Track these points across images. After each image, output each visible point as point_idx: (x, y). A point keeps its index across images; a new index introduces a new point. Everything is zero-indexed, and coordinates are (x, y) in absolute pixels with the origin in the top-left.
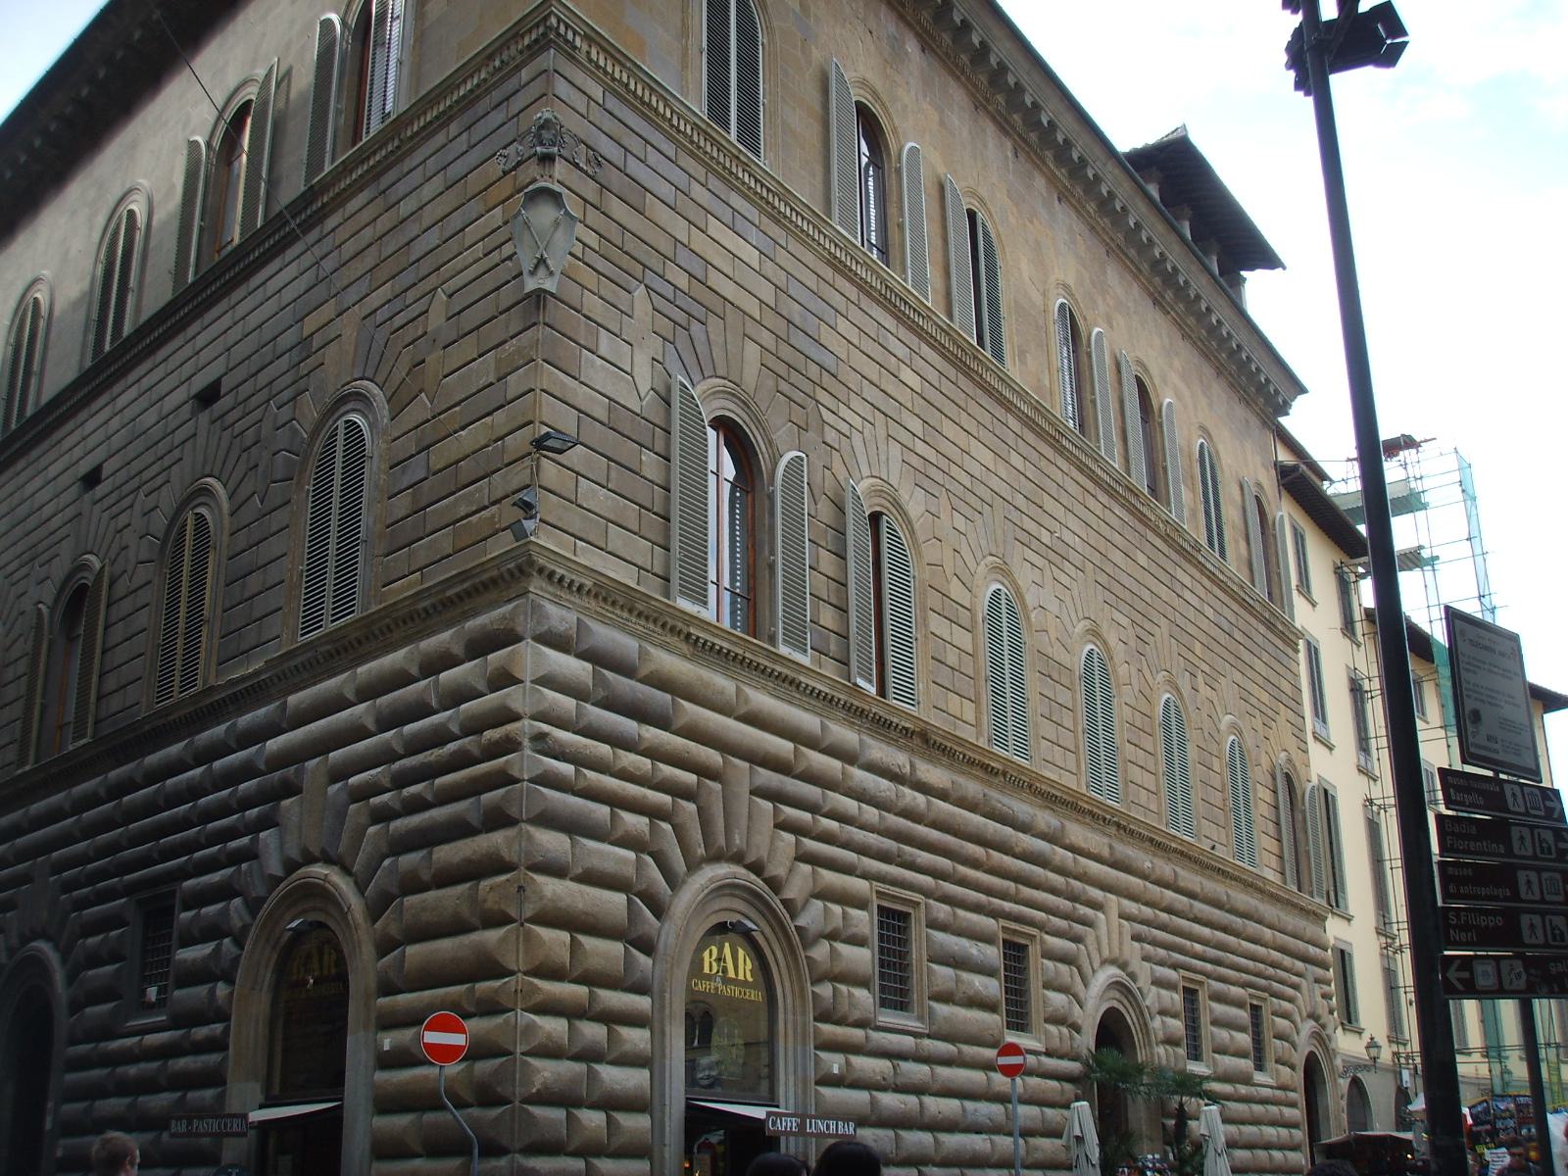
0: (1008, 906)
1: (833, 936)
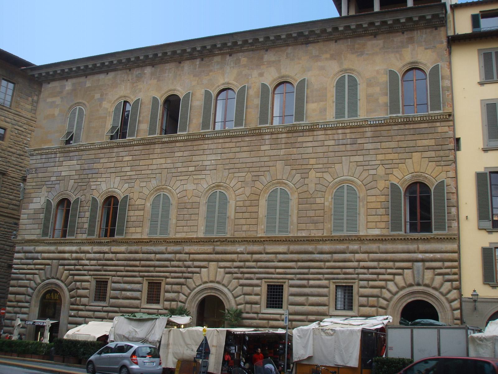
0: (146, 274)
1: (78, 289)
